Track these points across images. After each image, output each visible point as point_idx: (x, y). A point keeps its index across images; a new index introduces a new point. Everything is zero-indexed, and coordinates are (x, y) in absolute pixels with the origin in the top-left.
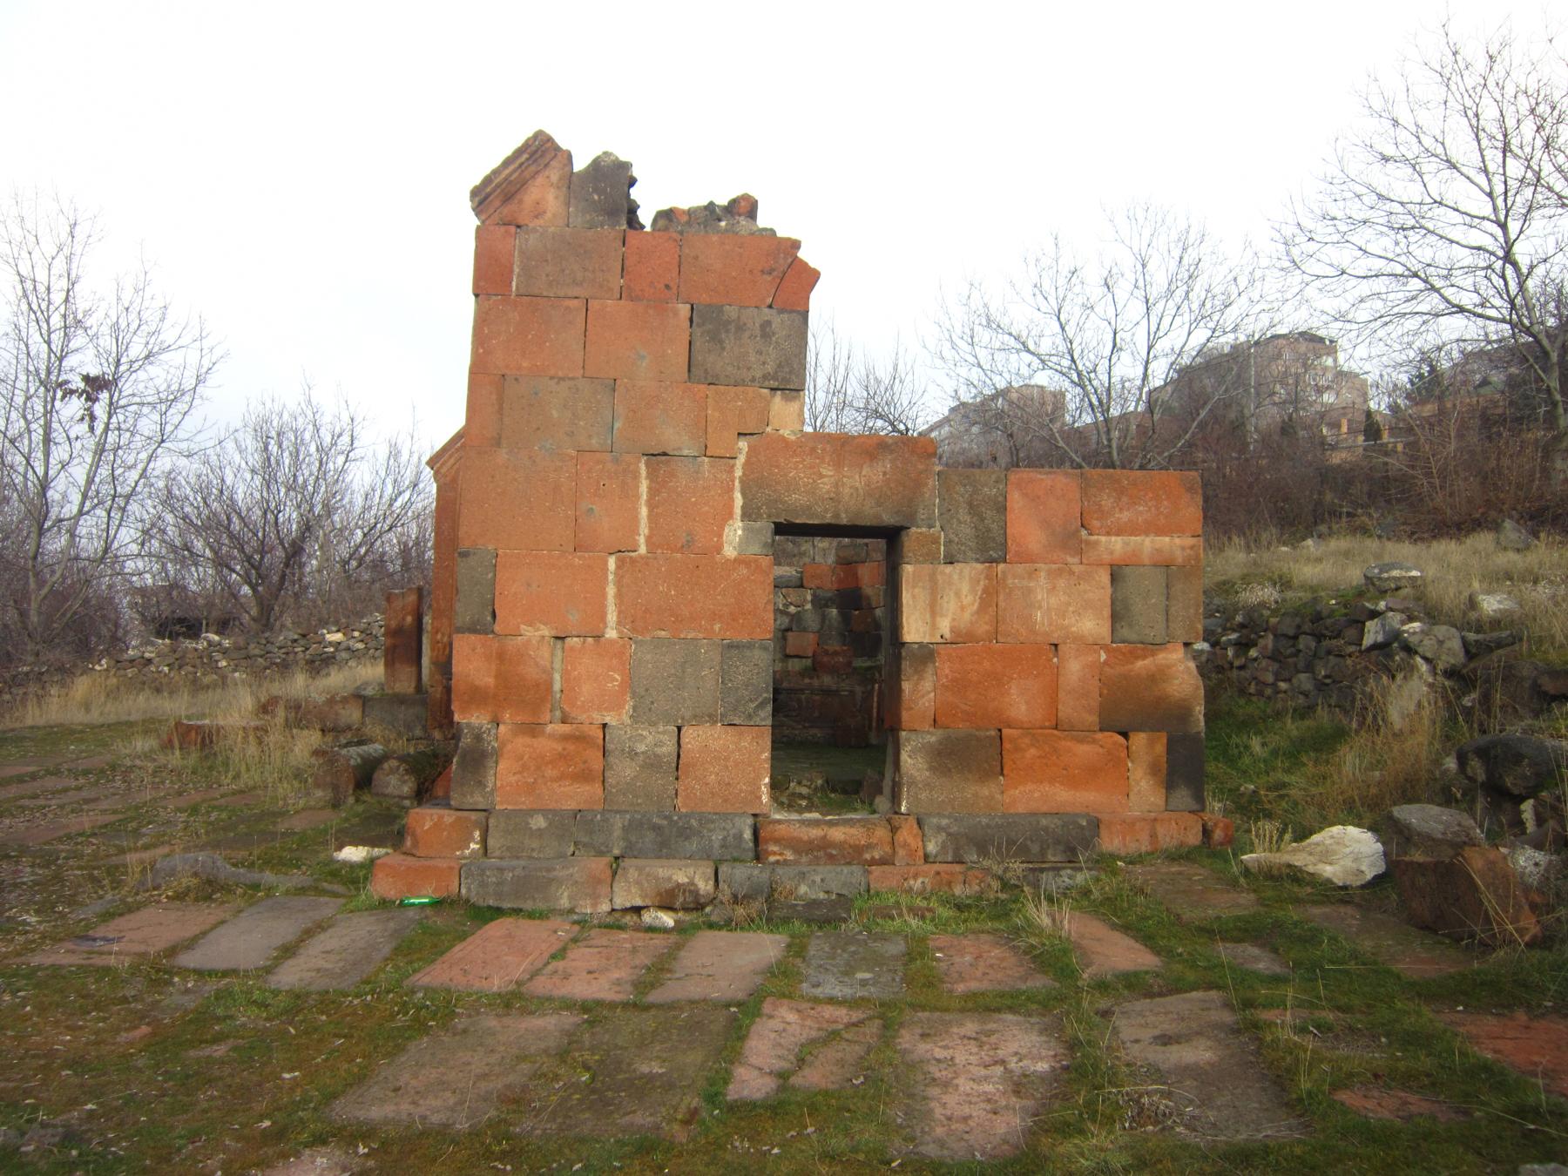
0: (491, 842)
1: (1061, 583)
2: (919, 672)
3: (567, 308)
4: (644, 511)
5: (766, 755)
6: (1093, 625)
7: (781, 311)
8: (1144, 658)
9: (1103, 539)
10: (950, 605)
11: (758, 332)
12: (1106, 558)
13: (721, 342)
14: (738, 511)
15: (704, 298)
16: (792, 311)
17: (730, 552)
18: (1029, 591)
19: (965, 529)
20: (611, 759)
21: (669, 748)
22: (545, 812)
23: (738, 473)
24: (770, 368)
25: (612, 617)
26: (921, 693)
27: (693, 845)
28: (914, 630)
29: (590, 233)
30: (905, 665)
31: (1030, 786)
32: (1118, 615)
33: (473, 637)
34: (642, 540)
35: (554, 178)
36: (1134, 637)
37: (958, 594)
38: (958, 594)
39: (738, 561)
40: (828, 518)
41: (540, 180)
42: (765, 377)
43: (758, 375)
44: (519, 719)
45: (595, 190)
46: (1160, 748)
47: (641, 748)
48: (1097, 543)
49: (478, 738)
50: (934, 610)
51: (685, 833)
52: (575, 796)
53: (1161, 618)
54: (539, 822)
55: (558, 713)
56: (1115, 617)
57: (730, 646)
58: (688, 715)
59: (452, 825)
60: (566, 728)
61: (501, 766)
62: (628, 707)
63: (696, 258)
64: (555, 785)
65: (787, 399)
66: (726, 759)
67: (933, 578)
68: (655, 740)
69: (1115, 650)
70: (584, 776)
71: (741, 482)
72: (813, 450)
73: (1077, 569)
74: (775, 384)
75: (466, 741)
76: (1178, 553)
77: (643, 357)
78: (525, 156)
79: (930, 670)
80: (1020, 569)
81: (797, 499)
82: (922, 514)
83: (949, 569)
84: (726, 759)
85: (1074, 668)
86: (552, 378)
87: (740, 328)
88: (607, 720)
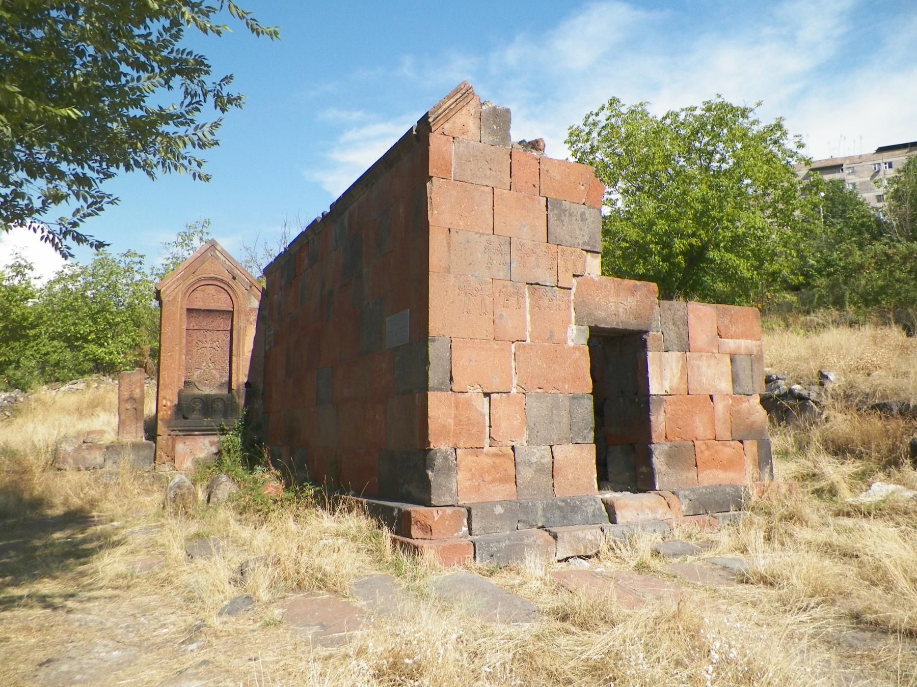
0: (474, 525)
2: (658, 411)
3: (483, 191)
4: (528, 317)
5: (594, 461)
6: (725, 385)
7: (589, 207)
9: (726, 340)
10: (668, 374)
11: (579, 218)
13: (562, 221)
14: (573, 320)
15: (552, 195)
16: (594, 208)
17: (571, 344)
18: (699, 367)
19: (672, 335)
20: (518, 468)
22: (501, 503)
23: (572, 297)
24: (586, 239)
25: (515, 382)
26: (659, 421)
27: (579, 517)
28: (655, 388)
29: (493, 148)
30: (652, 407)
31: (708, 471)
32: (735, 380)
33: (439, 393)
34: (528, 334)
35: (472, 112)
36: (741, 391)
37: (671, 369)
38: (671, 369)
39: (575, 348)
40: (614, 325)
41: (464, 111)
42: (584, 243)
44: (468, 445)
45: (494, 123)
46: (755, 449)
47: (534, 460)
49: (446, 458)
50: (662, 376)
51: (575, 509)
52: (504, 491)
53: (750, 381)
54: (499, 510)
55: (488, 440)
56: (734, 381)
57: (574, 398)
58: (556, 438)
59: (451, 516)
60: (493, 450)
61: (461, 476)
62: (525, 437)
63: (547, 171)
64: (491, 486)
65: (592, 257)
66: (576, 464)
67: (660, 360)
68: (540, 454)
70: (503, 480)
71: (575, 303)
72: (606, 286)
73: (717, 355)
74: (588, 248)
75: (439, 461)
76: (754, 349)
77: (524, 226)
78: (460, 95)
79: (662, 410)
80: (695, 355)
81: (601, 314)
82: (654, 324)
84: (576, 464)
85: (720, 406)
86: (476, 233)
87: (571, 215)
88: (514, 444)
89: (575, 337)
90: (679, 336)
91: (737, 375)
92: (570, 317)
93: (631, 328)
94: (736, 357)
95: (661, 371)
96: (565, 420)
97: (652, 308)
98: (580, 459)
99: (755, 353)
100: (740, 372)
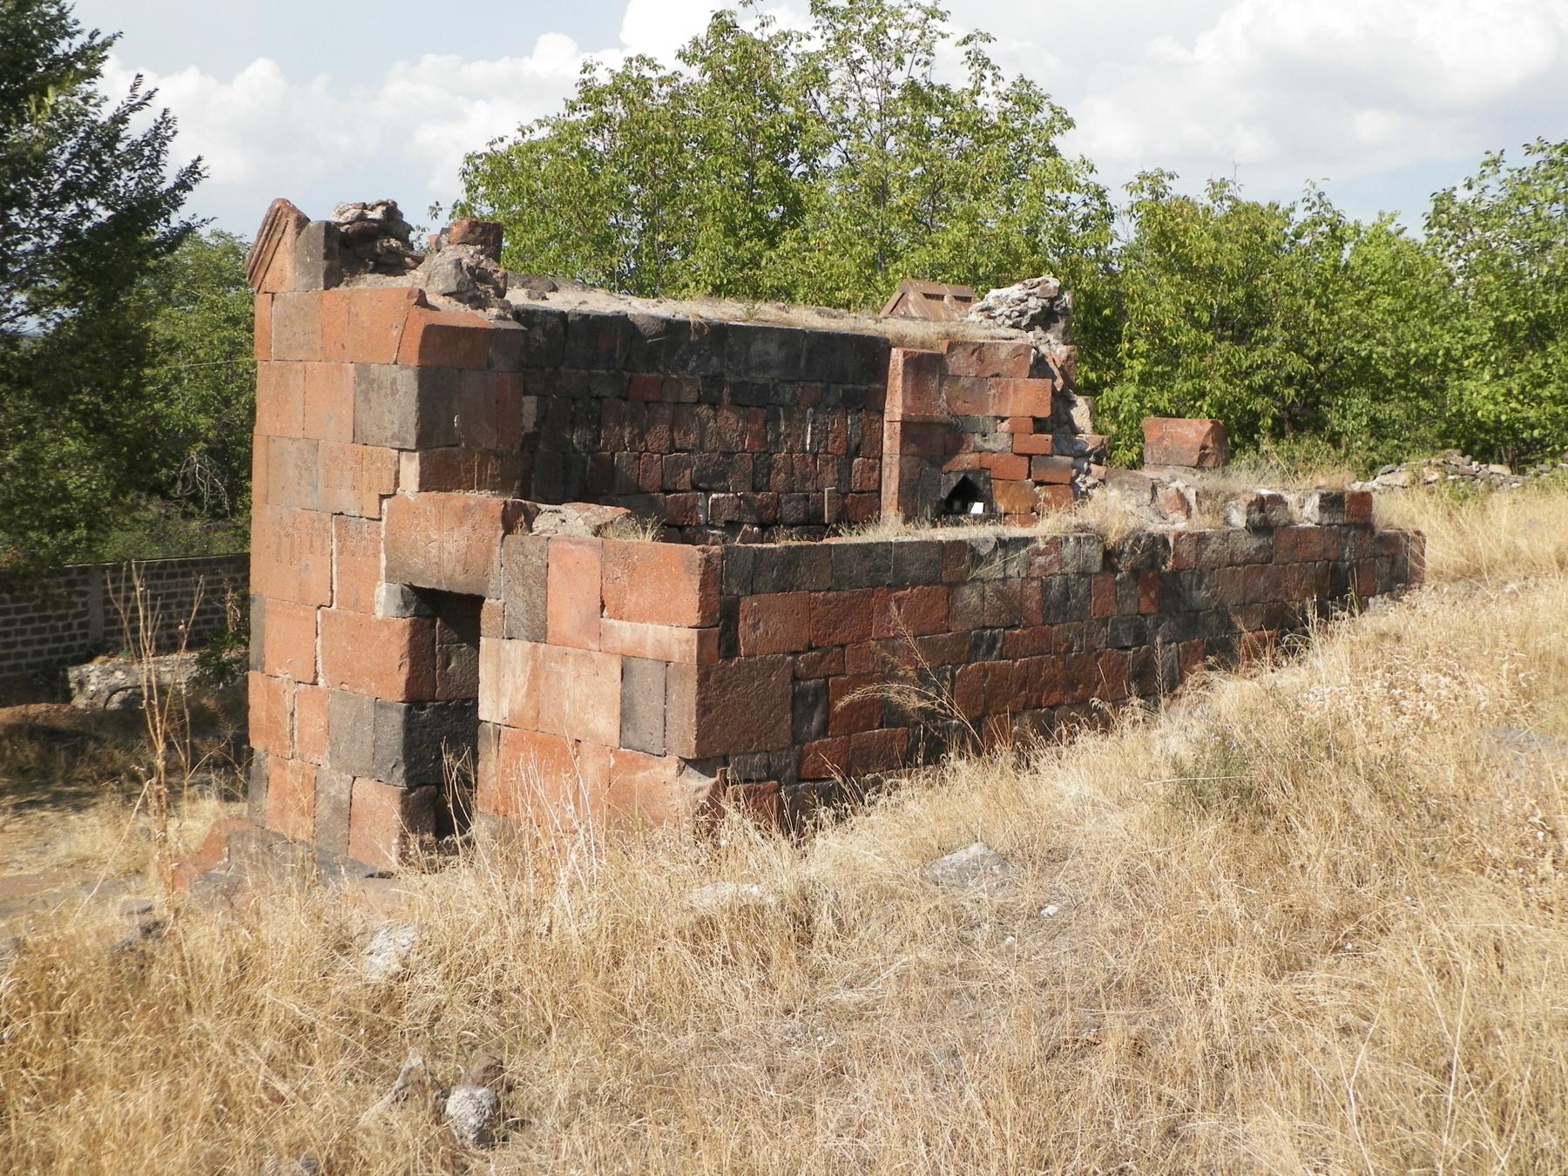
1: (584, 671)
8: (645, 768)
9: (616, 623)
10: (508, 686)
12: (618, 650)
14: (383, 572)
16: (408, 367)
21: (345, 797)
32: (626, 716)
36: (636, 743)
39: (385, 623)
43: (389, 435)
48: (612, 627)
53: (660, 724)
69: (624, 755)
73: (596, 656)
80: (556, 650)
81: (418, 563)
83: (507, 644)
89: (384, 600)
90: (531, 609)
91: (632, 706)
92: (377, 567)
93: (457, 590)
94: (634, 662)
95: (498, 678)
96: (368, 740)
97: (490, 552)
98: (381, 803)
99: (676, 658)
100: (640, 700)
